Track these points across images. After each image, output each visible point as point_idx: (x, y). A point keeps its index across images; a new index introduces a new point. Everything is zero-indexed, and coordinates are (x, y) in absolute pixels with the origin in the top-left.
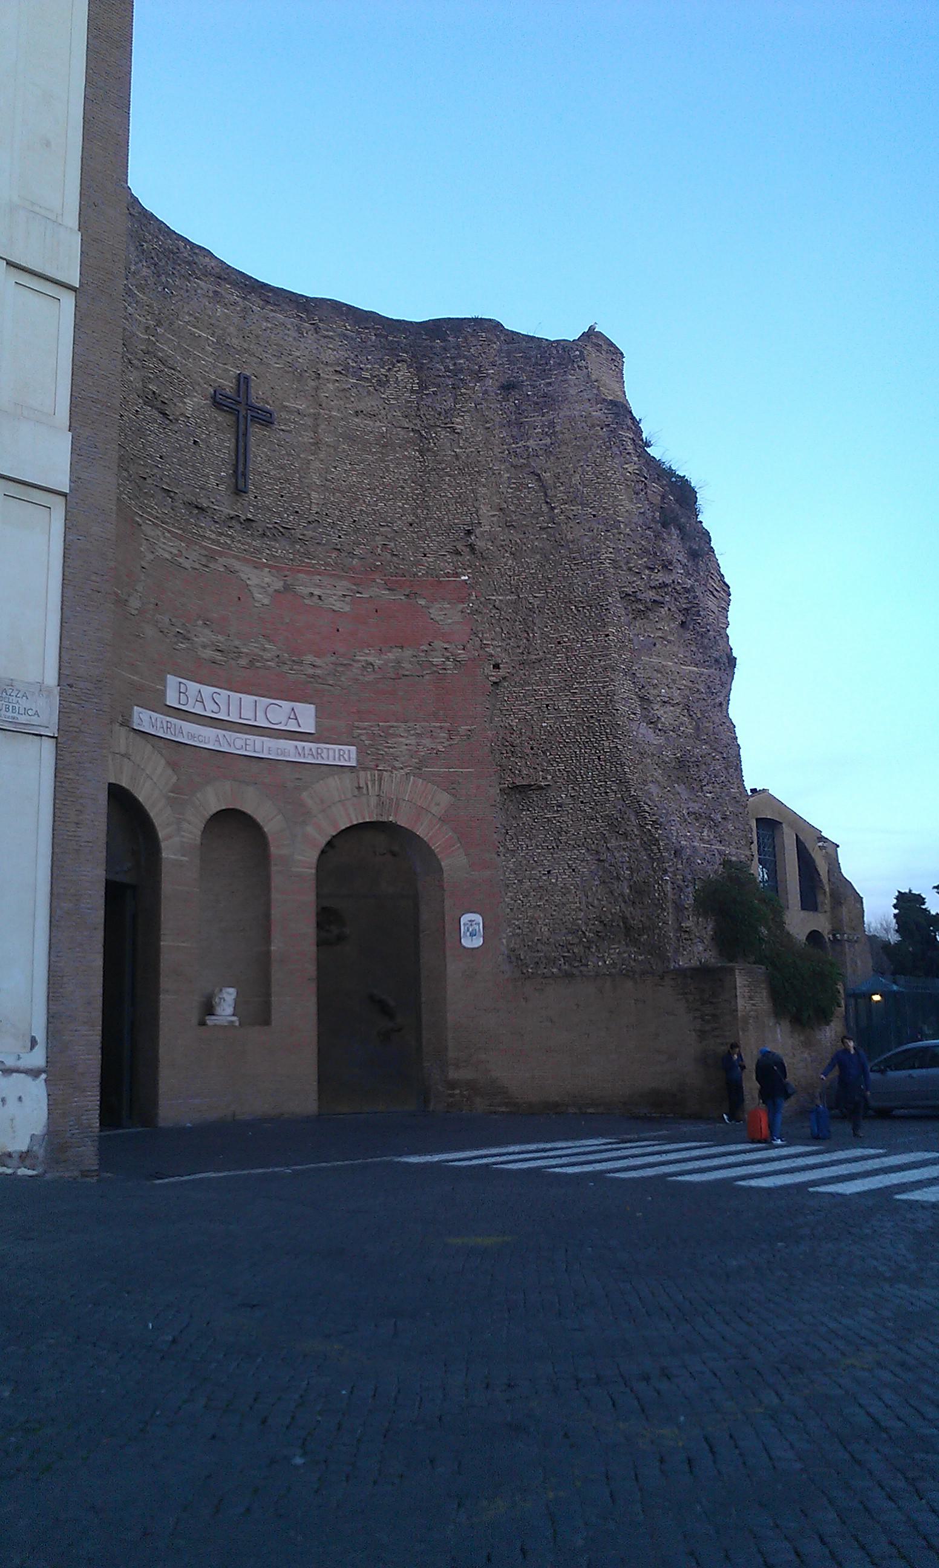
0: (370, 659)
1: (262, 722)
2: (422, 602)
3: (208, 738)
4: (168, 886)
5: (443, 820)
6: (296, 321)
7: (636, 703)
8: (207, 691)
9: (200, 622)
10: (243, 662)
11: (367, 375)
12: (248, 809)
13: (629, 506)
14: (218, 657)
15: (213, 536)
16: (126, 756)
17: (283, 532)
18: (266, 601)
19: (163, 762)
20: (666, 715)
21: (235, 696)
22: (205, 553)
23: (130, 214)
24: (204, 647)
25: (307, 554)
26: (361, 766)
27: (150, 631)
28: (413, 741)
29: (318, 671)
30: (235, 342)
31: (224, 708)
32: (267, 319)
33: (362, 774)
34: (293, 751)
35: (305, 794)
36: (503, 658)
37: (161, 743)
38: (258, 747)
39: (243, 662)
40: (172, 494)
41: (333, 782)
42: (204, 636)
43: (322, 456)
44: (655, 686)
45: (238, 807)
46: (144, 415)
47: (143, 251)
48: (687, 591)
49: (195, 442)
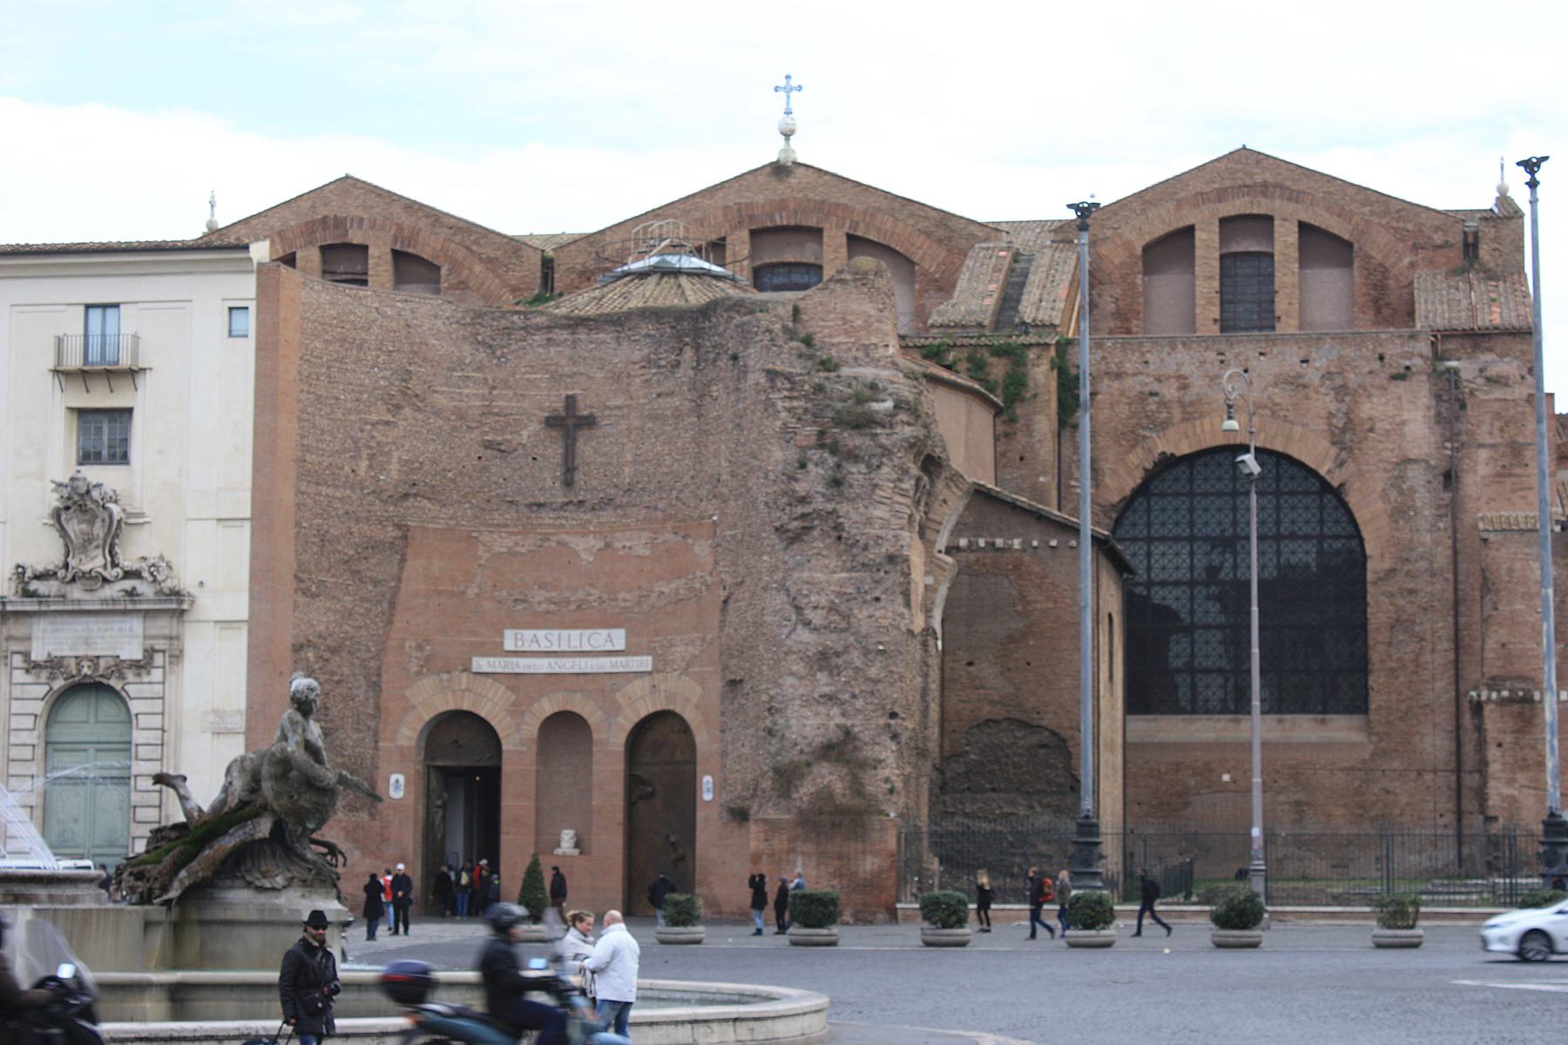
0: (662, 589)
1: (586, 647)
2: (690, 541)
3: (543, 665)
4: (507, 768)
5: (697, 707)
6: (615, 334)
7: (790, 611)
8: (541, 633)
11: (663, 363)
12: (577, 710)
13: (778, 454)
17: (608, 502)
18: (591, 559)
19: (503, 688)
20: (817, 618)
21: (565, 633)
24: (540, 603)
25: (626, 516)
26: (656, 670)
27: (488, 605)
28: (683, 648)
29: (628, 604)
30: (567, 370)
31: (555, 643)
32: (591, 342)
33: (656, 675)
34: (608, 665)
35: (618, 696)
36: (729, 580)
38: (583, 665)
39: (573, 607)
41: (637, 683)
42: (539, 595)
43: (633, 437)
44: (806, 596)
47: (479, 342)
48: (829, 513)
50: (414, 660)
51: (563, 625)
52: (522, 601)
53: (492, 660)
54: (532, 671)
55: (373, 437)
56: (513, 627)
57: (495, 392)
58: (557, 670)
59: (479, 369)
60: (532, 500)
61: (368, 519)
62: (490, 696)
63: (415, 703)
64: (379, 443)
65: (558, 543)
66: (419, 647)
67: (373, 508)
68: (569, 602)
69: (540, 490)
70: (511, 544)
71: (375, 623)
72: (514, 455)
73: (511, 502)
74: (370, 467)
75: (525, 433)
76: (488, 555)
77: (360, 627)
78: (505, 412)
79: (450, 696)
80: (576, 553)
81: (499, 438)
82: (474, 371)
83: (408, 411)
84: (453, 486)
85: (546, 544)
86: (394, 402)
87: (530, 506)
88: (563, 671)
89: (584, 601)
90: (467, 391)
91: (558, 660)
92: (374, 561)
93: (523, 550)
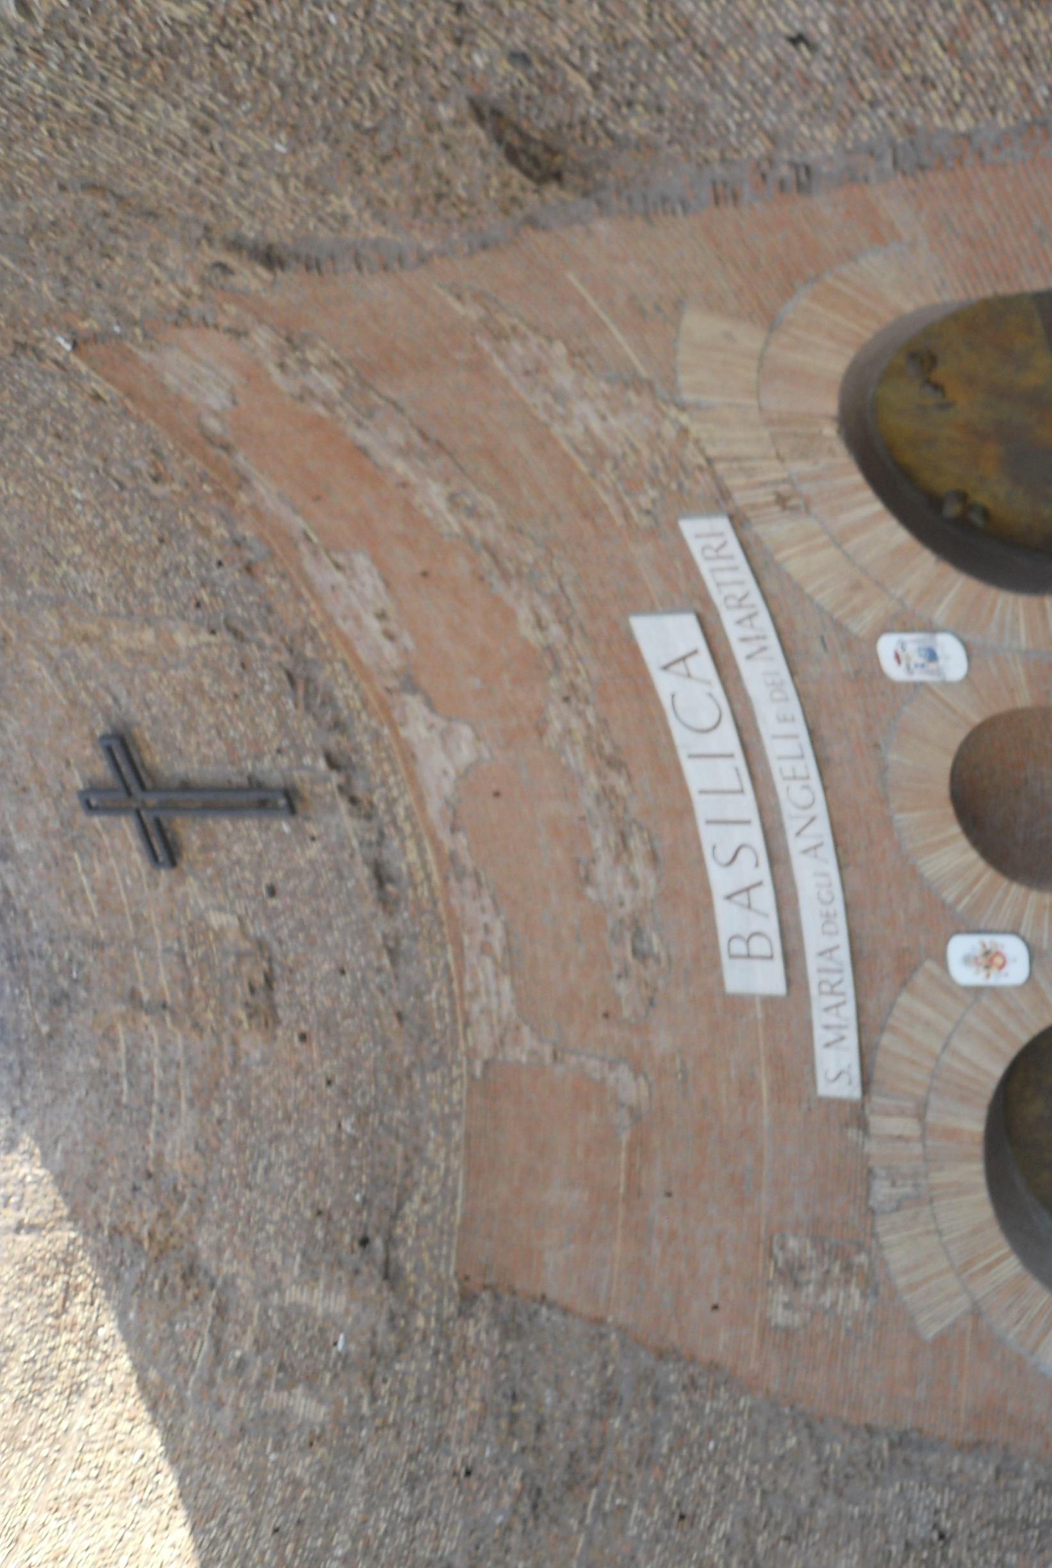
1: (727, 738)
8: (721, 880)
9: (590, 892)
10: (619, 782)
14: (636, 842)
15: (410, 844)
16: (920, 1114)
19: (904, 999)
21: (703, 808)
22: (453, 883)
23: (23, 1072)
24: (633, 882)
27: (663, 1041)
31: (738, 835)
37: (871, 1005)
39: (619, 782)
40: (391, 944)
45: (943, 788)
46: (297, 1022)
49: (272, 891)
50: (827, 1299)
51: (683, 810)
52: (638, 934)
53: (820, 1036)
54: (838, 906)
55: (242, 1364)
56: (716, 965)
57: (146, 996)
58: (822, 827)
59: (109, 1036)
60: (372, 895)
61: (440, 1406)
62: (937, 1046)
63: (962, 1303)
64: (260, 1346)
65: (454, 829)
66: (791, 1275)
67: (411, 1383)
68: (606, 794)
69: (341, 877)
70: (488, 962)
71: (720, 1417)
72: (275, 946)
73: (393, 954)
74: (311, 1381)
75: (216, 919)
76: (526, 1030)
77: (725, 1482)
78: (178, 972)
79: (938, 1177)
80: (467, 776)
81: (241, 990)
82: (115, 1049)
83: (204, 1240)
84: (373, 1119)
85: (469, 863)
86: (177, 1280)
87: (387, 903)
88: (820, 808)
89: (594, 751)
90: (157, 1070)
91: (791, 826)
92: (549, 1398)
93: (498, 931)
